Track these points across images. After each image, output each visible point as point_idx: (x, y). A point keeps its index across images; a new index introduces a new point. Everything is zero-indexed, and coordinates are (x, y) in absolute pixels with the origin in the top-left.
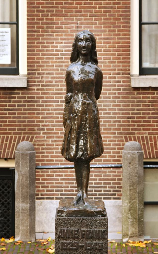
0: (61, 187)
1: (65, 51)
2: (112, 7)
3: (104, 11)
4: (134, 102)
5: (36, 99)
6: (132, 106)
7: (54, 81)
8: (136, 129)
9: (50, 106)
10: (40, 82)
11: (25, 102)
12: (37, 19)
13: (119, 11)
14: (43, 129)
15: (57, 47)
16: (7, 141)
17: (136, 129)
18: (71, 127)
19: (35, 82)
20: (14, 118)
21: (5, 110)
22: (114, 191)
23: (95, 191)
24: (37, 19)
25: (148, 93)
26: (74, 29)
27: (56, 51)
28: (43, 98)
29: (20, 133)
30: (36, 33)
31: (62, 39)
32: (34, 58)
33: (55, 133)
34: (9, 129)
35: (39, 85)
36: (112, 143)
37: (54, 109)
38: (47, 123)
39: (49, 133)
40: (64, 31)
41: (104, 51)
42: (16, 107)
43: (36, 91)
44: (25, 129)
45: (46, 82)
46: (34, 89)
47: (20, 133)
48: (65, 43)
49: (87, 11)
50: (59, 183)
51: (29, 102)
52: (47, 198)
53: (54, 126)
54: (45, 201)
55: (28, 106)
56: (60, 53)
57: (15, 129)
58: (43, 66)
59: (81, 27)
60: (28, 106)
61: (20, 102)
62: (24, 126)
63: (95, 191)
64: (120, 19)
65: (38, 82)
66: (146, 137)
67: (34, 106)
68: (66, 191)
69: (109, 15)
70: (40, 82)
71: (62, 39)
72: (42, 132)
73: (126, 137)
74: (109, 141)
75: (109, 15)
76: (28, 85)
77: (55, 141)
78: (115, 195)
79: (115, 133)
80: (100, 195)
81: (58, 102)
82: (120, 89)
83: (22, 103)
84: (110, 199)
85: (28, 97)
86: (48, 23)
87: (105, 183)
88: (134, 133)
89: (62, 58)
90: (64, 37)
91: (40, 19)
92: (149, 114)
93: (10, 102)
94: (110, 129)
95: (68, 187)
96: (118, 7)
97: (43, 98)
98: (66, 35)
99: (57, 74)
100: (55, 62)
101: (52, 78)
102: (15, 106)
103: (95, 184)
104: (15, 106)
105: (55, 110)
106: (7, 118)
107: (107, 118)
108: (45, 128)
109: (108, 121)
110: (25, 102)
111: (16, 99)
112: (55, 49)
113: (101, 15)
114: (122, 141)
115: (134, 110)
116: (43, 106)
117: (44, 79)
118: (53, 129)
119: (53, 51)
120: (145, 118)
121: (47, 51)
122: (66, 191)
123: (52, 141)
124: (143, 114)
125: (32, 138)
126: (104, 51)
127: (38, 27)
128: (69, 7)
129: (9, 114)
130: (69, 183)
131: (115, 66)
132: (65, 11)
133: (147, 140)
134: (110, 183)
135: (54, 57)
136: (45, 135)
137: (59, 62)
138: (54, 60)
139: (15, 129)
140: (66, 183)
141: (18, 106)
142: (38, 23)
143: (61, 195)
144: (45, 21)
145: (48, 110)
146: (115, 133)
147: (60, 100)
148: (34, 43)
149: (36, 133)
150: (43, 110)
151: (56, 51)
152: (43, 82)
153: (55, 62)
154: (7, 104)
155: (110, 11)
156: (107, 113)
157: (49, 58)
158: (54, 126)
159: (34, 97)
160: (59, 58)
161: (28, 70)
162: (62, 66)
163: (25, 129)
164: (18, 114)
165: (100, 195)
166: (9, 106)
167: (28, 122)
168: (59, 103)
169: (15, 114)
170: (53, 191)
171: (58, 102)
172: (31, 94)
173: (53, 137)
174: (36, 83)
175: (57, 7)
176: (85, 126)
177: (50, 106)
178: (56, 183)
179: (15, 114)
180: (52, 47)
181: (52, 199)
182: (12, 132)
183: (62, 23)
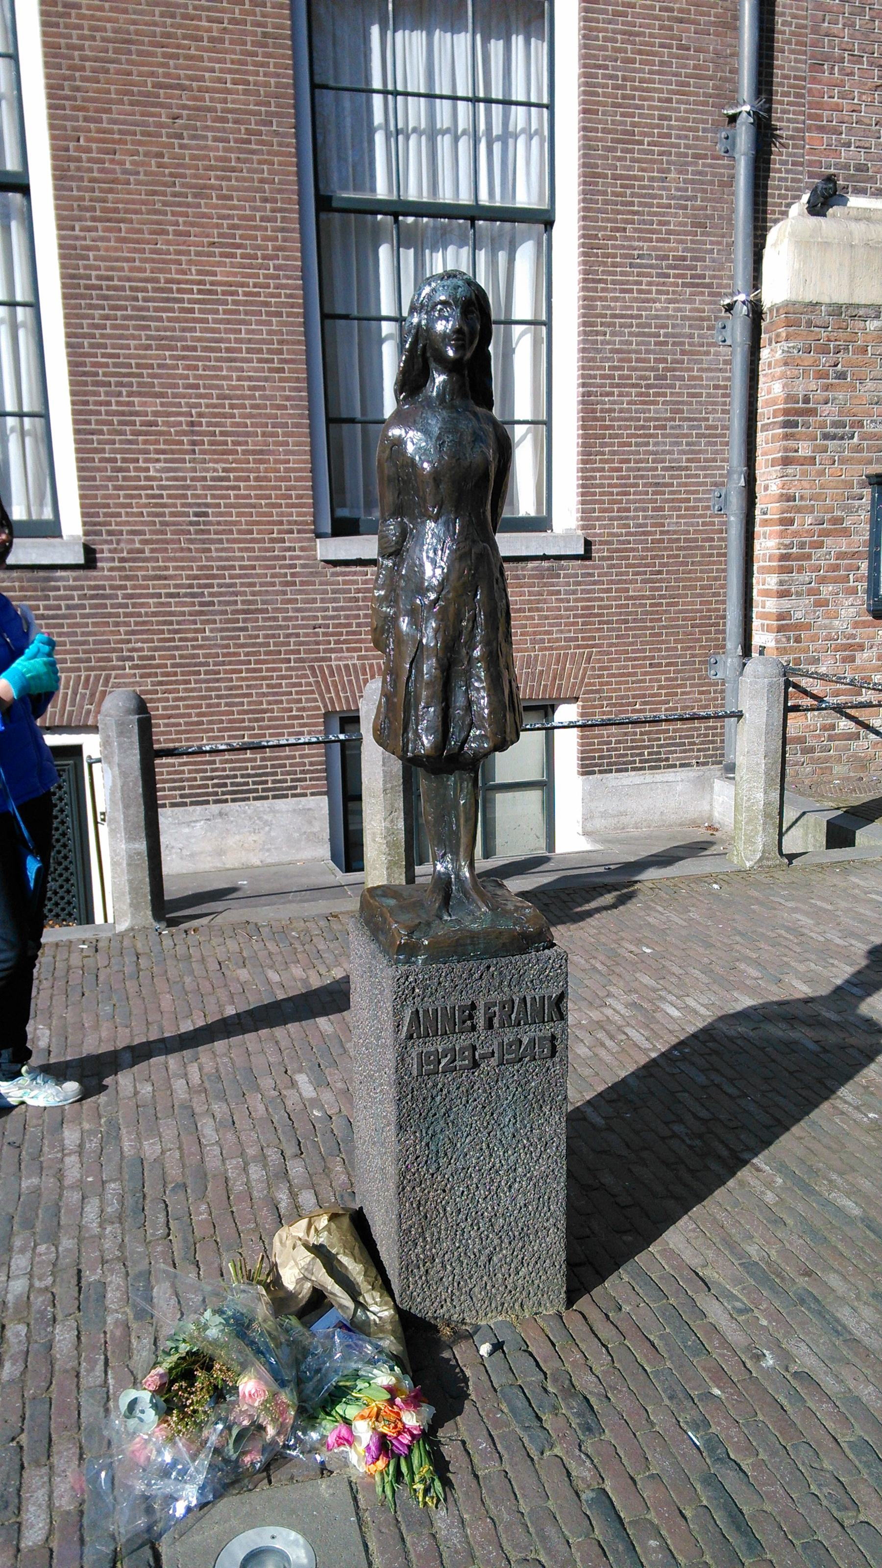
0: (182, 780)
1: (168, 479)
2: (266, 379)
3: (251, 388)
4: (325, 592)
5: (108, 591)
6: (323, 601)
7: (147, 548)
8: (332, 651)
9: (142, 605)
10: (115, 551)
12: (97, 403)
13: (283, 389)
14: (131, 659)
15: (147, 470)
17: (332, 651)
18: (421, 641)
22: (292, 780)
23: (254, 783)
24: (97, 403)
25: (355, 573)
26: (185, 427)
27: (148, 479)
28: (125, 587)
29: (78, 669)
30: (95, 437)
31: (158, 452)
32: (95, 497)
36: (284, 682)
39: (144, 667)
40: (161, 433)
41: (257, 479)
42: (63, 611)
44: (89, 660)
47: (78, 669)
48: (166, 461)
49: (211, 387)
50: (176, 772)
51: (93, 597)
53: (156, 649)
56: (155, 483)
58: (119, 515)
59: (200, 424)
60: (92, 607)
61: (72, 598)
62: (85, 652)
63: (254, 783)
64: (285, 408)
65: (110, 551)
66: (354, 665)
67: (105, 606)
68: (191, 787)
69: (262, 397)
70: (115, 551)
71: (158, 452)
72: (128, 664)
73: (312, 668)
74: (278, 678)
75: (262, 397)
77: (161, 683)
78: (295, 788)
79: (288, 661)
80: (264, 790)
81: (159, 596)
82: (294, 566)
83: (76, 601)
84: (286, 796)
85: (91, 588)
86: (123, 414)
87: (273, 766)
88: (330, 659)
89: (161, 496)
90: (162, 447)
91: (101, 404)
92: (358, 617)
93: (47, 598)
94: (279, 653)
95: (195, 779)
96: (282, 380)
97: (125, 587)
98: (166, 442)
99: (153, 532)
100: (146, 506)
102: (59, 608)
103: (253, 768)
104: (59, 608)
105: (155, 614)
107: (271, 628)
108: (135, 654)
109: (273, 636)
111: (62, 592)
112: (142, 474)
113: (243, 397)
114: (306, 676)
115: (326, 609)
116: (126, 606)
117: (122, 545)
118: (153, 658)
119: (138, 479)
120: (349, 625)
121: (125, 479)
122: (191, 787)
124: (347, 617)
126: (257, 479)
127: (98, 422)
128: (169, 376)
130: (197, 771)
131: (281, 514)
132: (162, 385)
133: (356, 672)
134: (285, 766)
135: (143, 492)
137: (156, 505)
138: (144, 501)
140: (190, 772)
142: (99, 413)
143: (182, 796)
144: (114, 408)
145: (139, 615)
146: (289, 661)
147: (163, 591)
148: (93, 460)
149: (114, 668)
150: (126, 615)
151: (148, 479)
152: (122, 551)
153: (146, 506)
154: (41, 603)
155: (263, 388)
156: (269, 619)
157: (132, 497)
158: (156, 649)
160: (153, 497)
161: (85, 524)
162: (163, 515)
164: (70, 626)
165: (264, 790)
166: (47, 608)
167: (95, 642)
168: (163, 600)
169: (62, 626)
171: (159, 596)
172: (95, 578)
175: (141, 375)
177: (142, 605)
180: (137, 469)
183: (156, 414)
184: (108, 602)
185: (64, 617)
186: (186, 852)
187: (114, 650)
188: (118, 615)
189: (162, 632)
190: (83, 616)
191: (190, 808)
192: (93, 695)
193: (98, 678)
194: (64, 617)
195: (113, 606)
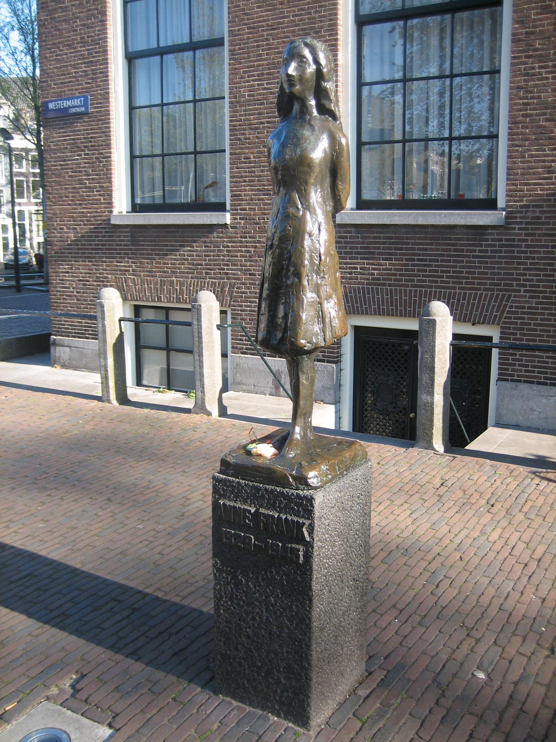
9: (536, 252)
11: (500, 246)
14: (525, 286)
16: (474, 300)
19: (515, 218)
20: (485, 268)
21: (474, 257)
28: (526, 240)
29: (493, 290)
33: (541, 292)
34: (478, 284)
35: (521, 223)
37: (542, 257)
38: (531, 277)
43: (517, 231)
44: (499, 285)
45: (533, 218)
46: (515, 229)
47: (493, 290)
51: (505, 246)
52: (525, 382)
54: (523, 386)
55: (506, 252)
57: (485, 284)
60: (506, 252)
61: (495, 246)
65: (521, 218)
67: (513, 252)
72: (522, 289)
76: (507, 223)
77: (541, 303)
81: (547, 247)
85: (507, 240)
93: (481, 245)
97: (526, 240)
101: (541, 212)
104: (486, 251)
105: (543, 259)
106: (476, 267)
110: (500, 246)
116: (526, 252)
118: (538, 286)
123: (537, 303)
125: (510, 296)
129: (479, 262)
136: (528, 294)
139: (485, 284)
141: (492, 251)
143: (545, 378)
145: (533, 258)
150: (526, 258)
152: (528, 218)
159: (513, 240)
163: (499, 285)
164: (492, 263)
166: (480, 251)
167: (505, 274)
169: (487, 262)
170: (533, 372)
171: (547, 247)
172: (510, 234)
173: (538, 297)
174: (518, 220)
176: (288, 271)
177: (536, 252)
178: (539, 362)
179: (487, 262)
181: (532, 382)
182: (482, 287)
184: (516, 249)
185: (489, 257)
186: (542, 415)
187: (516, 280)
188: (520, 258)
189: (546, 270)
190: (500, 257)
191: (548, 387)
192: (499, 306)
193: (503, 296)
194: (489, 257)
195: (519, 252)
